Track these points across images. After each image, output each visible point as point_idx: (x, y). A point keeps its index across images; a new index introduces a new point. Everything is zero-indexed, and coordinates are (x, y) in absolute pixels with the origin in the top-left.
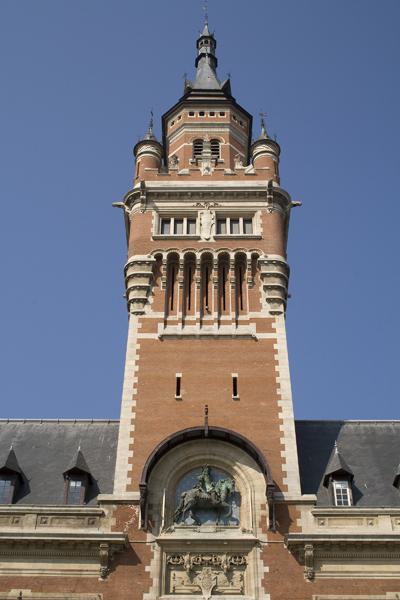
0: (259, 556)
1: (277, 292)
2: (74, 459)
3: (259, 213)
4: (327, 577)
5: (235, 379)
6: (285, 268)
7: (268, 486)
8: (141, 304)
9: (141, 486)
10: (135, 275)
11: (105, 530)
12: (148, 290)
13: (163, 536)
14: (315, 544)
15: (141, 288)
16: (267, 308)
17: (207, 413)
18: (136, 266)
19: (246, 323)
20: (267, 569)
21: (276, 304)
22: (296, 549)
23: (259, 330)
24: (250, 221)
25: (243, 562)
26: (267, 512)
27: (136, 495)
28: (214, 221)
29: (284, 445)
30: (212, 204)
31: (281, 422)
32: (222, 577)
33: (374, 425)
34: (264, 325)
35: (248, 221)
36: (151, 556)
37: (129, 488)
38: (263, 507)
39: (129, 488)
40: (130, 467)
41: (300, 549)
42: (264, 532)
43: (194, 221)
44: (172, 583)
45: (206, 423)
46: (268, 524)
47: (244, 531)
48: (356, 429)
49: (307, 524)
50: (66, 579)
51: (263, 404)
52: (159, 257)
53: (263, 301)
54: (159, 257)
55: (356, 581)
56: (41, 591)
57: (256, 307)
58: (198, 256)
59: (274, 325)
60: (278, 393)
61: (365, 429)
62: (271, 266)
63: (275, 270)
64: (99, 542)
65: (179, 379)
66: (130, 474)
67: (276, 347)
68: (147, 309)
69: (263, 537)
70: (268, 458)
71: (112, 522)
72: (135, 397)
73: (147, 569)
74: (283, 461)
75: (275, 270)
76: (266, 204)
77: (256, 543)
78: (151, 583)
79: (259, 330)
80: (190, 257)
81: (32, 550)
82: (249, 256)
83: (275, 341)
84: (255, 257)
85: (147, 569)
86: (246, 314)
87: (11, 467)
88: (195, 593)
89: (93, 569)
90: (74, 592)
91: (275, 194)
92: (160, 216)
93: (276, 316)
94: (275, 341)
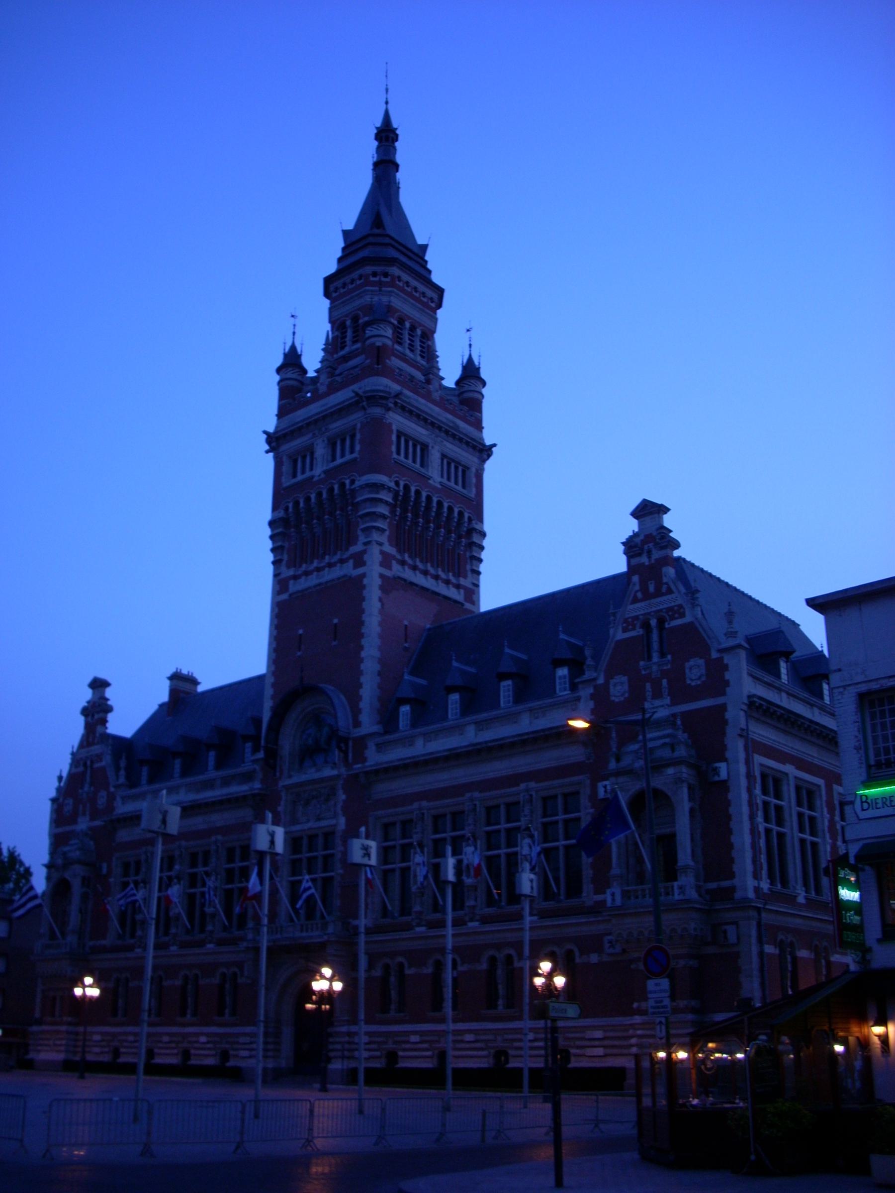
3: (359, 426)
11: (257, 785)
23: (356, 567)
52: (287, 509)
53: (359, 532)
54: (287, 509)
58: (313, 496)
69: (343, 770)
79: (356, 567)
80: (308, 499)
82: (347, 482)
83: (364, 575)
84: (353, 482)
94: (364, 575)
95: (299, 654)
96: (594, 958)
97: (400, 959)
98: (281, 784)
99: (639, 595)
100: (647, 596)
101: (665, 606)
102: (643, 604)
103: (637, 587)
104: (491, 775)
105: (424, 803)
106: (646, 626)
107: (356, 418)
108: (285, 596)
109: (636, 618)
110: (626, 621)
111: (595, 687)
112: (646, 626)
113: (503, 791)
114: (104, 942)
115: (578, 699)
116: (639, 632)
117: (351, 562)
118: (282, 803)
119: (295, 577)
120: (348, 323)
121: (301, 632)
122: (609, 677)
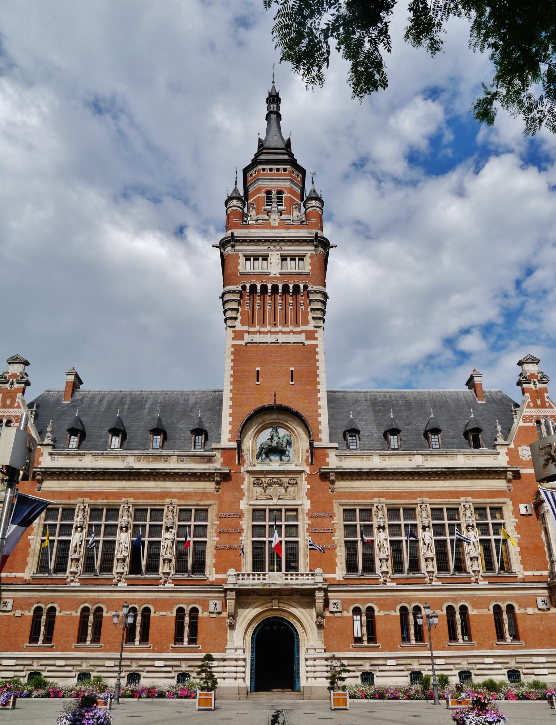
0: (304, 479)
1: (319, 312)
2: (197, 422)
4: (342, 490)
5: (292, 371)
6: (326, 296)
7: (310, 441)
8: (234, 320)
9: (237, 441)
10: (229, 309)
11: (217, 465)
12: (238, 301)
13: (251, 469)
14: (336, 473)
15: (233, 309)
16: (312, 323)
17: (275, 395)
18: (230, 294)
19: (300, 333)
20: (309, 486)
21: (317, 320)
22: (324, 476)
23: (307, 338)
24: (303, 259)
25: (295, 482)
26: (309, 454)
27: (234, 445)
28: (280, 260)
29: (320, 414)
30: (278, 248)
31: (319, 399)
32: (283, 491)
33: (375, 393)
34: (311, 335)
35: (302, 259)
36: (244, 479)
37: (230, 440)
38: (307, 451)
39: (230, 440)
40: (230, 428)
41: (328, 476)
42: (307, 466)
43: (266, 259)
44: (255, 494)
45: (275, 402)
46: (310, 461)
47: (296, 465)
48: (365, 395)
49: (333, 462)
50: (196, 493)
51: (308, 387)
52: (244, 287)
53: (310, 318)
54: (244, 287)
55: (357, 492)
56: (183, 499)
57: (306, 323)
58: (269, 286)
59: (316, 335)
60: (318, 380)
61: (371, 395)
62: (315, 294)
63: (319, 297)
64: (214, 473)
65: (258, 371)
66: (230, 432)
67: (317, 350)
68: (237, 323)
69: (307, 469)
70: (310, 421)
71: (221, 460)
72: (232, 383)
73: (242, 487)
74: (320, 423)
75: (319, 297)
76: (313, 248)
77: (303, 471)
78: (244, 494)
79: (307, 338)
81: (176, 477)
82: (302, 286)
83: (317, 346)
84: (306, 287)
85: (242, 487)
86: (299, 327)
87: (159, 427)
88: (269, 499)
89: (209, 486)
90: (201, 500)
91: (320, 241)
92: (244, 256)
93: (317, 329)
94: (317, 346)
95: (257, 383)
96: (530, 610)
97: (370, 604)
98: (243, 469)
99: (531, 404)
100: (536, 406)
101: (549, 414)
102: (535, 410)
103: (529, 400)
104: (438, 489)
105: (383, 500)
106: (538, 422)
107: (309, 249)
108: (243, 343)
109: (532, 416)
110: (524, 416)
111: (508, 449)
112: (538, 422)
113: (447, 500)
114: (19, 575)
115: (498, 454)
116: (533, 424)
117: (303, 335)
118: (246, 483)
119: (249, 333)
120: (274, 192)
121: (258, 369)
122: (517, 445)
